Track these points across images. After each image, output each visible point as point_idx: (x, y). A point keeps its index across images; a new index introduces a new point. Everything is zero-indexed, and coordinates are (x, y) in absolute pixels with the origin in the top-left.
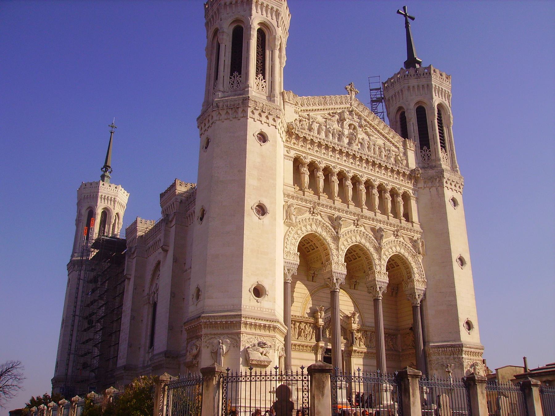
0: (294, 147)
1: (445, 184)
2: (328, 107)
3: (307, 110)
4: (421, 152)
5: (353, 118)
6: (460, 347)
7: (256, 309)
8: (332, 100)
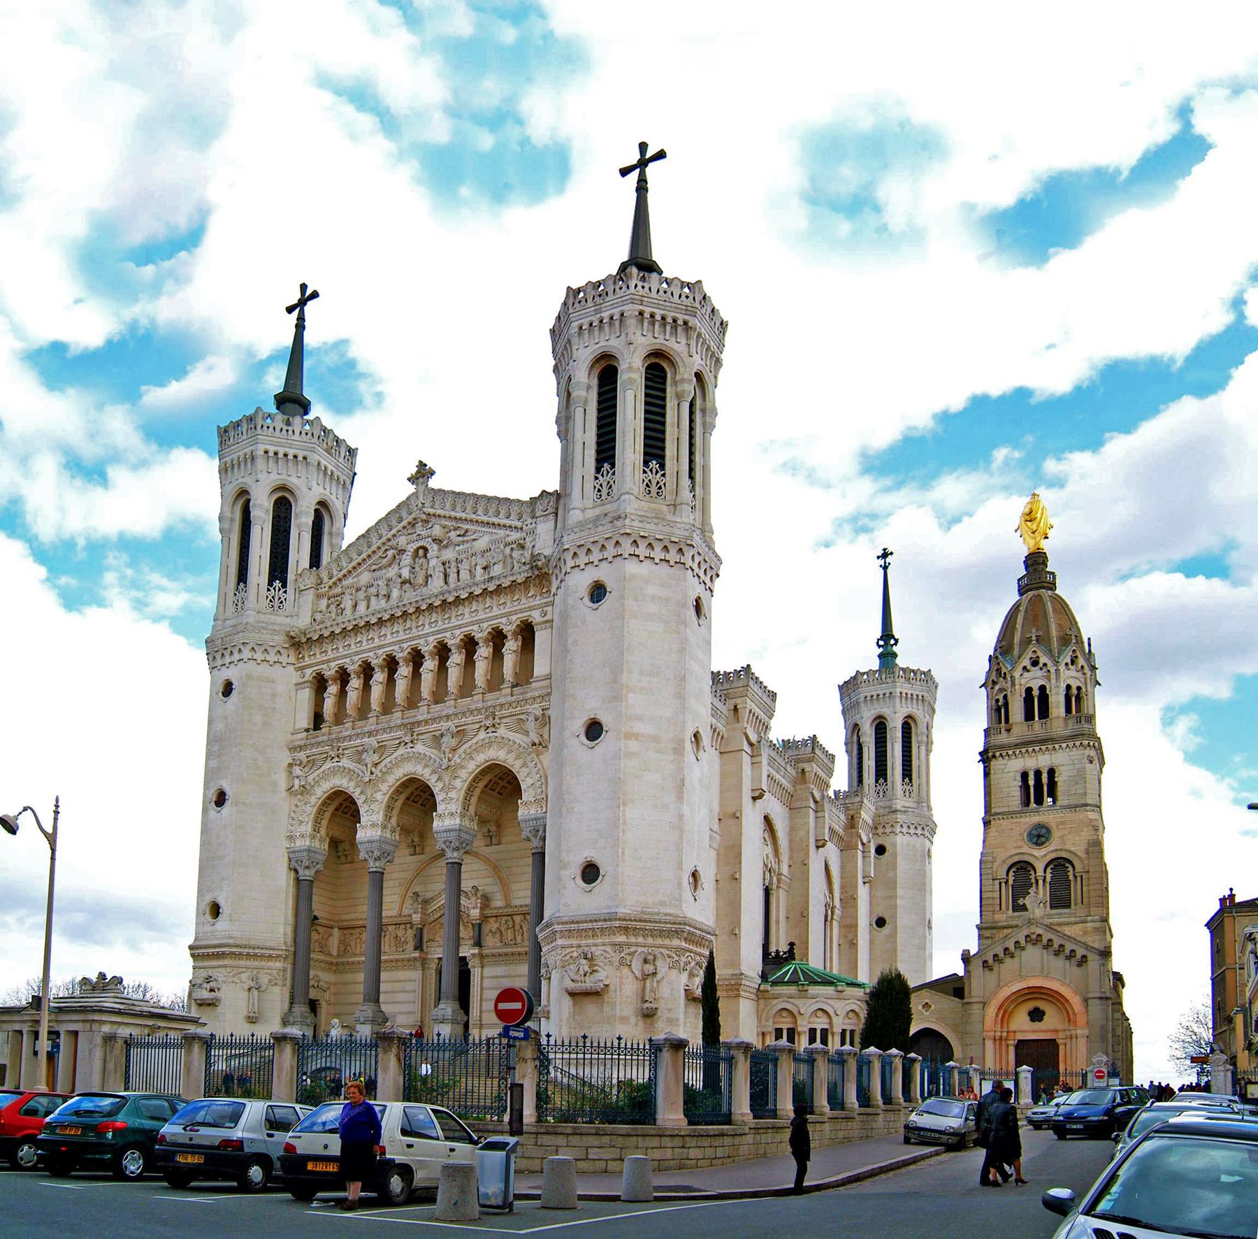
2: (374, 548)
3: (340, 580)
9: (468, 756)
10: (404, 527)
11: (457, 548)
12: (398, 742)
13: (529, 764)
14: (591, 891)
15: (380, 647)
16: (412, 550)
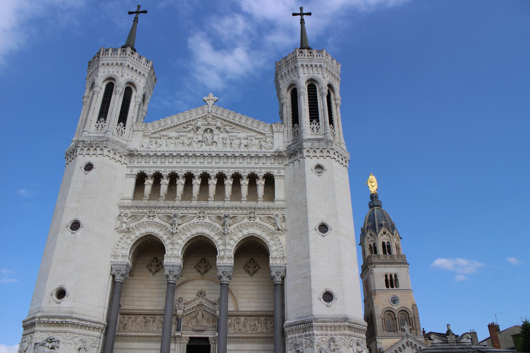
0: (138, 165)
3: (159, 131)
4: (293, 130)
5: (209, 123)
6: (309, 322)
7: (54, 309)
8: (186, 115)
9: (239, 230)
10: (199, 118)
11: (230, 134)
12: (194, 215)
13: (275, 239)
14: (330, 306)
15: (184, 167)
16: (204, 129)
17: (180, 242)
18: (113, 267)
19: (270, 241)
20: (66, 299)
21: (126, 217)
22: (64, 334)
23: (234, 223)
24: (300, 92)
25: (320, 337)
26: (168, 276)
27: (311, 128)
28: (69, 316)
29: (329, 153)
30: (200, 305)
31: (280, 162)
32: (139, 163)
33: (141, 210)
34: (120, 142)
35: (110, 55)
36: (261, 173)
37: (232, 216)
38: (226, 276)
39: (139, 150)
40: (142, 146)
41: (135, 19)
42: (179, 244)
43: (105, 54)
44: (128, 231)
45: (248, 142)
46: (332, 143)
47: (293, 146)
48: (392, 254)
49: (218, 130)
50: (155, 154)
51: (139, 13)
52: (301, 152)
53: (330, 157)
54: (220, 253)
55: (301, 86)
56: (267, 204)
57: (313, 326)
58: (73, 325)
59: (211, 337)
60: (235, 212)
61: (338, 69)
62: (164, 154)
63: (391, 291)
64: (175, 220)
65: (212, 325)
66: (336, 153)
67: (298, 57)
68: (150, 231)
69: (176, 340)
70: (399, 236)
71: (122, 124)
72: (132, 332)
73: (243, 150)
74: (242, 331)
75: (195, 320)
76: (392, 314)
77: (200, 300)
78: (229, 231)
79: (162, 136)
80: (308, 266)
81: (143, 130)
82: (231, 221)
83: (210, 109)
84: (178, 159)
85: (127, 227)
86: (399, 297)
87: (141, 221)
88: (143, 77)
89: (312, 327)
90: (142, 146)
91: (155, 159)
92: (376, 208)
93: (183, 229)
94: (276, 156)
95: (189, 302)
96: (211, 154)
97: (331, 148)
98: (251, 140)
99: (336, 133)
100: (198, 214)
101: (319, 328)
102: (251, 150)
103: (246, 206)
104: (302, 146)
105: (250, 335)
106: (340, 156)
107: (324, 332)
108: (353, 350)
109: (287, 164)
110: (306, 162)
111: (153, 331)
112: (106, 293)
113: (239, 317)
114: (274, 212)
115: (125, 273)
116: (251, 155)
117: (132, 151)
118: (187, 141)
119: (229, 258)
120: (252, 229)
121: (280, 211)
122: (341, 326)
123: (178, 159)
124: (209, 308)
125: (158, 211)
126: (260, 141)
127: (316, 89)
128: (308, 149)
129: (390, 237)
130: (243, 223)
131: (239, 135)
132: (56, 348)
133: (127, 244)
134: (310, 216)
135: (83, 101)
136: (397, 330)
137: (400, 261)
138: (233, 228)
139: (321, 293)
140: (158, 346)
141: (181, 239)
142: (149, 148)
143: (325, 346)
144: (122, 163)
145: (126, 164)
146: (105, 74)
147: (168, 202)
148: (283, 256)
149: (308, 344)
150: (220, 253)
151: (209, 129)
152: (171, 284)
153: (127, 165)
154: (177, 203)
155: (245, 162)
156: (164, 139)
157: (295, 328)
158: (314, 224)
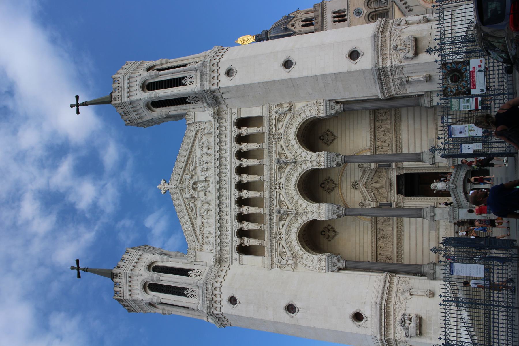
0: (230, 253)
1: (215, 87)
3: (196, 236)
4: (192, 103)
6: (379, 72)
7: (373, 322)
8: (179, 209)
9: (291, 149)
10: (182, 197)
13: (300, 112)
16: (193, 191)
17: (304, 206)
18: (330, 270)
19: (302, 118)
20: (363, 311)
21: (281, 261)
22: (397, 310)
23: (284, 154)
24: (155, 97)
25: (393, 60)
26: (338, 215)
27: (190, 84)
28: (380, 306)
29: (214, 64)
30: (366, 185)
31: (224, 113)
32: (228, 252)
33: (274, 247)
34: (208, 272)
35: (121, 289)
36: (236, 131)
37: (278, 156)
38: (336, 158)
39: (215, 253)
40: (211, 251)
41: (85, 271)
42: (307, 206)
43: (120, 294)
44: (294, 258)
45: (205, 146)
46: (204, 61)
47: (208, 100)
48: (314, 17)
49: (194, 177)
50: (219, 238)
51: (79, 267)
52: (214, 92)
53: (218, 63)
54: (314, 165)
55: (149, 97)
56: (266, 123)
57: (382, 67)
58: (388, 303)
59: (397, 173)
60: (273, 153)
61: (132, 63)
62: (219, 228)
63: (349, 16)
64: (283, 212)
65: (384, 173)
66: (215, 58)
67: (120, 102)
68: (295, 236)
69: (400, 207)
70: (296, 11)
71: (189, 273)
72: (393, 250)
73: (213, 150)
74: (390, 143)
75: (380, 190)
76: (371, 15)
77: (361, 186)
78: (293, 157)
79: (201, 232)
80: (325, 76)
81: (195, 251)
82: (283, 157)
83: (173, 186)
84: (223, 214)
85: (291, 259)
86: (355, 8)
87: (285, 247)
88: (142, 256)
89: (383, 68)
90: (211, 251)
91: (223, 237)
92: (270, 35)
93: (291, 203)
94: (219, 118)
95: (363, 197)
96: (218, 182)
97: (209, 62)
98: (203, 143)
99: (195, 60)
100: (277, 190)
101: (385, 62)
102: (213, 142)
103: (267, 143)
104: (208, 90)
105: (394, 135)
106: (217, 54)
107: (388, 56)
108: (405, 28)
109: (226, 106)
110: (224, 86)
111: (392, 230)
112: (356, 275)
113: (376, 147)
114: (273, 116)
115: (336, 258)
116: (218, 142)
117: (216, 260)
118: (205, 207)
119: (319, 156)
120: (289, 136)
121: (272, 109)
122: (382, 40)
123: (223, 214)
124: (368, 177)
125: (274, 230)
126: (204, 135)
127: (151, 83)
128: (211, 85)
129: (297, 20)
130: (285, 145)
131: (199, 155)
132: (410, 317)
133: (308, 258)
134: (276, 78)
135: (168, 314)
136: (387, 9)
137: (320, 9)
138: (290, 154)
139: (350, 62)
140: (406, 219)
141: (301, 205)
142: (213, 244)
143: (402, 55)
144: (228, 269)
145: (229, 265)
146: (140, 293)
147: (265, 220)
148: (316, 104)
149: (400, 72)
150: (314, 165)
151: (192, 186)
152: (346, 212)
153: (230, 264)
154: (266, 211)
155: (225, 147)
156: (203, 230)
157: (385, 86)
158: (284, 74)
